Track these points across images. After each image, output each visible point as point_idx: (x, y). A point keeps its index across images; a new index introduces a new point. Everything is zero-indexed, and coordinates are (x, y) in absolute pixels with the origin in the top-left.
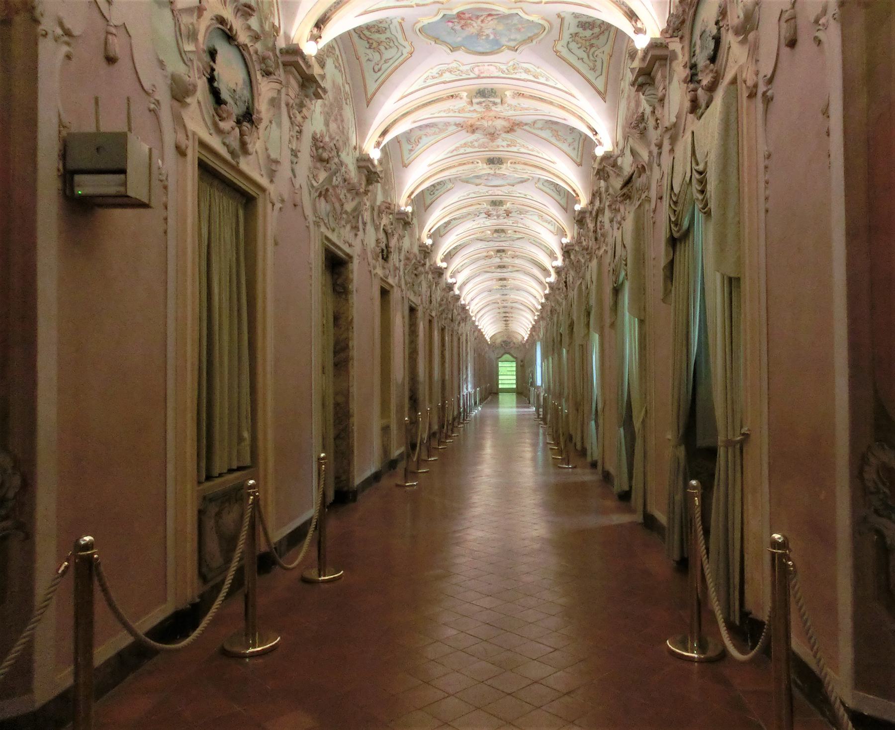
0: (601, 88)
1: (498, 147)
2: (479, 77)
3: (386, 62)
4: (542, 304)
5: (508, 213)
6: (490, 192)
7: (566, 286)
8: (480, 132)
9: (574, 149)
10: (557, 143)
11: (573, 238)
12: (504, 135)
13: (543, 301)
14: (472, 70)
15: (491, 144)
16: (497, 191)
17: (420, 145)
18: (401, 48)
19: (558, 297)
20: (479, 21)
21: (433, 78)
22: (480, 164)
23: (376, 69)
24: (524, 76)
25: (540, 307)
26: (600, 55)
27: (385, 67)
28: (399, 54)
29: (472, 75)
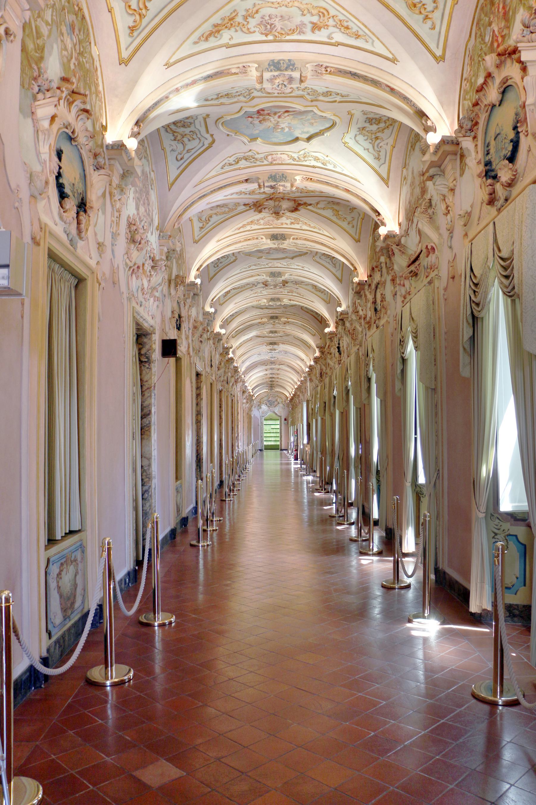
1: (282, 224)
2: (271, 164)
3: (188, 151)
4: (311, 367)
6: (270, 265)
8: (267, 210)
12: (289, 214)
13: (312, 363)
14: (266, 158)
15: (276, 221)
16: (277, 264)
17: (210, 223)
18: (202, 139)
21: (230, 165)
22: (264, 240)
23: (179, 157)
24: (313, 163)
26: (385, 146)
27: (186, 156)
28: (201, 145)
29: (266, 162)
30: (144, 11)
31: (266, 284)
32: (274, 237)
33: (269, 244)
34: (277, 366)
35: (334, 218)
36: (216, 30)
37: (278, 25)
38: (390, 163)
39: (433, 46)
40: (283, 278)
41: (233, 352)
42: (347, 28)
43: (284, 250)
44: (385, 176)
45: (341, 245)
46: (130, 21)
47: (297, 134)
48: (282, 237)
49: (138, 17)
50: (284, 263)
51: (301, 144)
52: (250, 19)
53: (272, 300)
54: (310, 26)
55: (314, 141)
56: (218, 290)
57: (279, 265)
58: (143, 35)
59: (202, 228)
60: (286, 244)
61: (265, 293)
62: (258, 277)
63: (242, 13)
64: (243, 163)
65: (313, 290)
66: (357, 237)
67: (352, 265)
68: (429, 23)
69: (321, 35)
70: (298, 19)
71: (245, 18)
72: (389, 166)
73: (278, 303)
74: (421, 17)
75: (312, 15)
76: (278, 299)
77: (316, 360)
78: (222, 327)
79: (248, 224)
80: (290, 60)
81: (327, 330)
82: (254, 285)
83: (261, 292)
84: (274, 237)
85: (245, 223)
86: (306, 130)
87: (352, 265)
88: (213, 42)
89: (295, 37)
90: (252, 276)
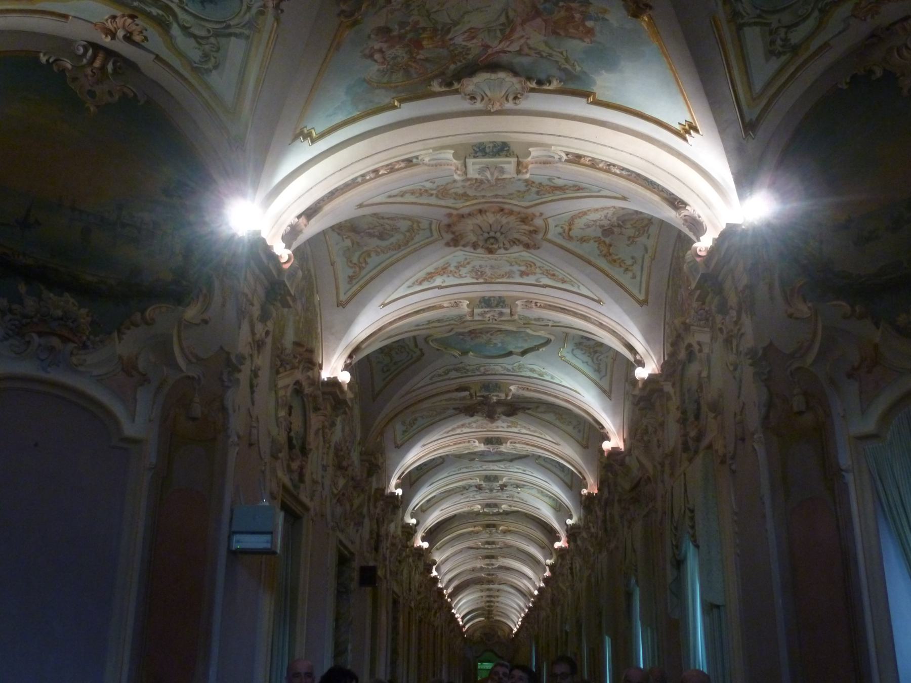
0: (607, 388)
2: (484, 374)
5: (503, 487)
6: (484, 467)
7: (572, 573)
9: (579, 431)
10: (564, 427)
11: (580, 519)
12: (504, 417)
13: (542, 585)
14: (478, 369)
15: (490, 425)
17: (415, 427)
19: (561, 585)
20: (488, 335)
21: (440, 375)
22: (477, 443)
23: (385, 369)
24: (529, 374)
25: (536, 593)
29: (478, 373)
30: (363, 265)
31: (479, 488)
32: (488, 441)
33: (482, 447)
34: (496, 586)
35: (557, 423)
36: (430, 276)
37: (488, 272)
38: (612, 371)
39: (635, 292)
40: (501, 482)
41: (437, 570)
42: (554, 275)
43: (501, 453)
44: (607, 388)
45: (567, 452)
46: (350, 272)
47: (511, 348)
48: (499, 441)
49: (357, 269)
50: (501, 466)
51: (514, 358)
52: (461, 268)
53: (488, 505)
54: (518, 273)
55: (528, 356)
56: (418, 499)
57: (495, 469)
58: (362, 282)
59: (405, 432)
60: (503, 448)
61: (478, 497)
62: (471, 481)
63: (454, 264)
64: (453, 374)
65: (539, 495)
66: (584, 443)
67: (580, 473)
68: (630, 274)
69: (531, 279)
70: (508, 268)
71: (457, 267)
72: (612, 376)
73: (495, 510)
74: (622, 269)
75: (520, 265)
76: (496, 505)
77: (546, 580)
78: (423, 539)
79: (458, 427)
80: (500, 297)
81: (557, 545)
82: (465, 488)
83: (474, 497)
84: (488, 441)
85: (455, 426)
86: (520, 345)
87: (580, 473)
88: (425, 285)
89: (505, 280)
90: (463, 480)
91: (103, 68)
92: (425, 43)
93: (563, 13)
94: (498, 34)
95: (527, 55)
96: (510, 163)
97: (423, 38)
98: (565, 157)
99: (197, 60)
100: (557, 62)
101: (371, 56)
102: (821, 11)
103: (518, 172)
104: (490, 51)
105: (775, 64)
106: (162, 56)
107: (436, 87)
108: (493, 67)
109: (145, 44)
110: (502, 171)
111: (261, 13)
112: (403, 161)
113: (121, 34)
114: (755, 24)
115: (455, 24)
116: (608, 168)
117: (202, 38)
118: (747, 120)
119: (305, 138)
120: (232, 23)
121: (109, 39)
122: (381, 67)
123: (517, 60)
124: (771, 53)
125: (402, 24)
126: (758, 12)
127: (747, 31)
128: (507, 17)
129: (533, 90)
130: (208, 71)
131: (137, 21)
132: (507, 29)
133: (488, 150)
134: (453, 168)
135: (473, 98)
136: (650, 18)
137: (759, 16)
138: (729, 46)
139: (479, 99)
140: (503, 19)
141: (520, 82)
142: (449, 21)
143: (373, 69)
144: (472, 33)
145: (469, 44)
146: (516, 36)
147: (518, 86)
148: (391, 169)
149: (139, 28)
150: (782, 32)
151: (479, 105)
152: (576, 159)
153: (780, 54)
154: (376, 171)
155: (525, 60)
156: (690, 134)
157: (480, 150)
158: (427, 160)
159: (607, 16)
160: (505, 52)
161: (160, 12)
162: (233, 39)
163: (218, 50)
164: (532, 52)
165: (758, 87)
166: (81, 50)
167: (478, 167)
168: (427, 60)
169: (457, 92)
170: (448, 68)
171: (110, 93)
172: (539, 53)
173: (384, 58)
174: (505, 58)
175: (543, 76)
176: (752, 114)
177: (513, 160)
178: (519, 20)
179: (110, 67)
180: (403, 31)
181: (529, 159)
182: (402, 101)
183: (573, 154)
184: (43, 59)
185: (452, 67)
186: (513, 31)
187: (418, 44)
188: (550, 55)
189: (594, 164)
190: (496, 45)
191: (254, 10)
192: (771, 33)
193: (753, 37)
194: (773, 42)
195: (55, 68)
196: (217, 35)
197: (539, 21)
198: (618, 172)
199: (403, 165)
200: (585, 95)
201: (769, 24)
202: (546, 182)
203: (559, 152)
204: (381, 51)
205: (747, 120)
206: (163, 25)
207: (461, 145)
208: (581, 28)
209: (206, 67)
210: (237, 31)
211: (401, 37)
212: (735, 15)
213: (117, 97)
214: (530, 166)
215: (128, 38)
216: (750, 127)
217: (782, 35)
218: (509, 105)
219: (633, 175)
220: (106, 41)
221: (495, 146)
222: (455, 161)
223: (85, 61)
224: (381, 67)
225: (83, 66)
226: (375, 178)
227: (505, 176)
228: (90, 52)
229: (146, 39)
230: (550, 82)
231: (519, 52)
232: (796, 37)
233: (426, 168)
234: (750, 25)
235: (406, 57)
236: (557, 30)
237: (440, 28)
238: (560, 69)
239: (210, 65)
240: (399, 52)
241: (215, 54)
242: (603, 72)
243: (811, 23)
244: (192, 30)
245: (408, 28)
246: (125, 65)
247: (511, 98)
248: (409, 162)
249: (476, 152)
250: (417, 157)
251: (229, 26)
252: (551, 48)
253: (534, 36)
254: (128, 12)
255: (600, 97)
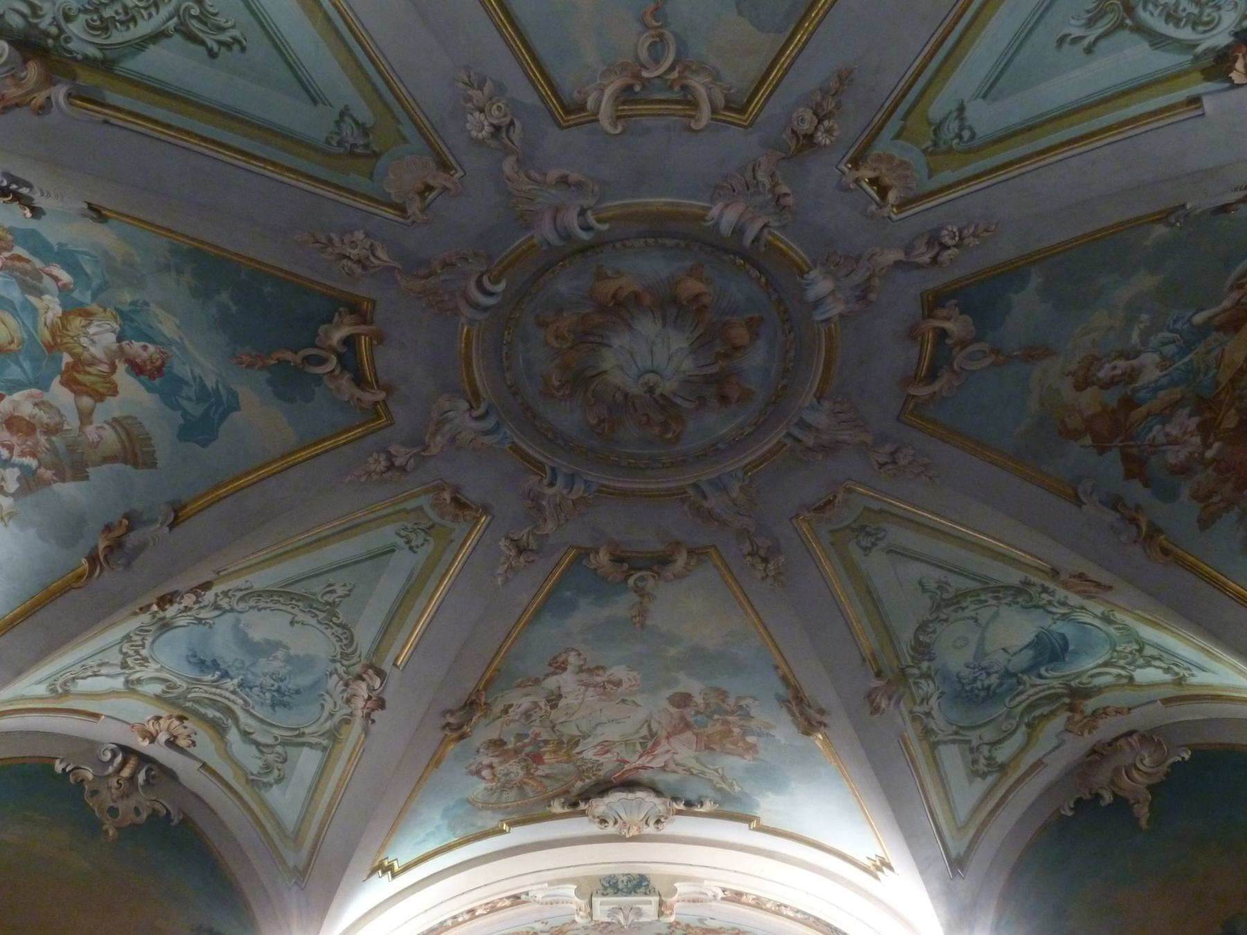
91: (132, 778)
92: (546, 757)
93: (719, 727)
94: (638, 748)
95: (674, 772)
96: (650, 903)
97: (545, 753)
98: (721, 894)
99: (255, 772)
100: (711, 781)
101: (478, 773)
102: (1029, 725)
103: (660, 914)
104: (627, 767)
105: (980, 786)
106: (210, 763)
107: (557, 807)
108: (629, 785)
109: (192, 750)
110: (639, 913)
111: (346, 721)
112: (508, 898)
113: (163, 737)
114: (953, 742)
115: (585, 736)
116: (778, 909)
117: (267, 746)
118: (953, 854)
119: (384, 872)
120: (307, 731)
121: (147, 742)
122: (489, 785)
123: (662, 779)
124: (975, 774)
125: (520, 737)
126: (954, 728)
127: (942, 749)
128: (650, 729)
129: (679, 812)
130: (268, 785)
131: (186, 723)
132: (650, 742)
133: (620, 886)
134: (574, 907)
135: (603, 821)
136: (825, 736)
137: (956, 733)
138: (924, 769)
139: (611, 823)
140: (644, 732)
141: (664, 803)
142: (576, 732)
143: (479, 788)
144: (606, 747)
145: (601, 759)
146: (658, 751)
147: (661, 808)
148: (493, 908)
149: (186, 732)
150: (985, 750)
151: (611, 829)
152: (736, 897)
153: (984, 775)
154: (471, 911)
155: (671, 778)
156: (882, 871)
157: (611, 886)
158: (540, 896)
159: (772, 732)
160: (645, 768)
161: (218, 715)
162: (306, 750)
163: (285, 760)
164: (680, 769)
165: (962, 815)
166: (109, 755)
167: (607, 907)
168: (547, 776)
169: (583, 813)
170: (573, 785)
171: (137, 811)
172: (689, 771)
173: (494, 775)
174: (644, 775)
175: (692, 797)
176: (957, 848)
177: (654, 899)
178: (664, 734)
179: (141, 777)
180: (519, 744)
181: (676, 897)
182: (512, 824)
183: (732, 891)
184: (59, 767)
185: (579, 784)
186: (656, 744)
187: (537, 758)
188: (703, 773)
189: (759, 904)
190: (634, 760)
191: (337, 718)
192: (972, 750)
193: (951, 757)
194: (975, 762)
195: (72, 779)
196: (285, 743)
197: (688, 735)
198: (791, 914)
199: (508, 903)
200: (747, 819)
201: (969, 742)
202: (695, 923)
203: (713, 887)
204: (491, 766)
205: (953, 854)
206: (219, 729)
207: (585, 877)
208: (741, 744)
209: (265, 780)
210: (313, 740)
211: (517, 751)
212: (927, 732)
213: (144, 816)
214: (676, 906)
215: (171, 743)
216: (957, 864)
217: (986, 753)
218: (650, 830)
219: (812, 919)
220: (143, 745)
221: (629, 881)
222: (577, 899)
223: (111, 769)
224: (489, 785)
225: (109, 776)
226: (470, 919)
227: (643, 919)
228: (119, 758)
229: (194, 743)
230: (702, 804)
231: (664, 769)
232: (1002, 754)
233: (537, 906)
234: (945, 743)
235: (522, 773)
236: (708, 745)
237: (565, 741)
238: (715, 788)
239: (271, 779)
240: (515, 769)
241: (280, 766)
242: (769, 794)
243: (1018, 739)
244: (254, 736)
245: (526, 741)
246: (160, 774)
247: (652, 822)
248: (516, 899)
249: (605, 888)
250: (527, 893)
251: (303, 734)
252: (703, 765)
253: (683, 751)
254: (178, 712)
255: (765, 822)
